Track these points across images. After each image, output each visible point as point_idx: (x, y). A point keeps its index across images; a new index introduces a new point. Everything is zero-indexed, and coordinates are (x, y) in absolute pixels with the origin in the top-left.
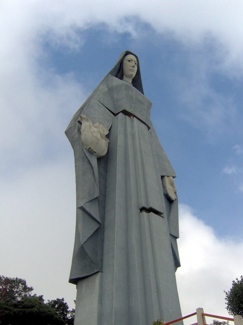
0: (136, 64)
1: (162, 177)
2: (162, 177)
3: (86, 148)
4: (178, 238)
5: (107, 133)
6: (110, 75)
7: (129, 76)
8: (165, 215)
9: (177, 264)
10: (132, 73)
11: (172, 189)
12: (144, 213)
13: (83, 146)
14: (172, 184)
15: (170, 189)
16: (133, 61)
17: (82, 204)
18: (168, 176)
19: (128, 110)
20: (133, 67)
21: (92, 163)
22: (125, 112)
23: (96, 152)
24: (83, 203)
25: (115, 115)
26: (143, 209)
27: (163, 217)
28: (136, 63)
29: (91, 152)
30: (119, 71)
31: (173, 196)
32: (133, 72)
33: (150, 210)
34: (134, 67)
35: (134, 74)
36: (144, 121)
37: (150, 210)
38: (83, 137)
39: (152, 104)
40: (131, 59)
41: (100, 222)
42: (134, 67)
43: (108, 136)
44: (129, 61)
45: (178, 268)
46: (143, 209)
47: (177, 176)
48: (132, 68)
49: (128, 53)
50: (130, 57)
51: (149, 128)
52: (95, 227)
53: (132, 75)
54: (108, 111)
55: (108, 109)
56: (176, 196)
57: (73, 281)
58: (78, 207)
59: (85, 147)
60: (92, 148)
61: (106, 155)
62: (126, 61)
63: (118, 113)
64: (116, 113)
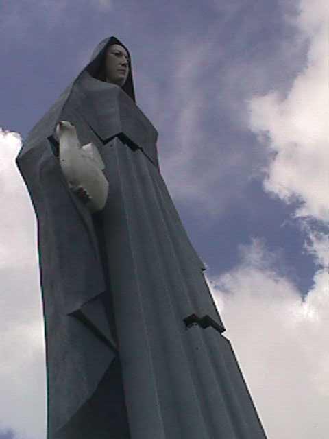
3: (71, 189)
6: (87, 74)
10: (123, 76)
12: (196, 328)
16: (124, 58)
20: (123, 65)
22: (122, 138)
25: (105, 142)
26: (189, 321)
29: (82, 196)
30: (99, 68)
32: (124, 74)
35: (125, 77)
44: (117, 54)
46: (189, 321)
48: (123, 68)
49: (113, 41)
50: (117, 48)
53: (122, 79)
60: (85, 190)
62: (112, 55)
63: (112, 138)
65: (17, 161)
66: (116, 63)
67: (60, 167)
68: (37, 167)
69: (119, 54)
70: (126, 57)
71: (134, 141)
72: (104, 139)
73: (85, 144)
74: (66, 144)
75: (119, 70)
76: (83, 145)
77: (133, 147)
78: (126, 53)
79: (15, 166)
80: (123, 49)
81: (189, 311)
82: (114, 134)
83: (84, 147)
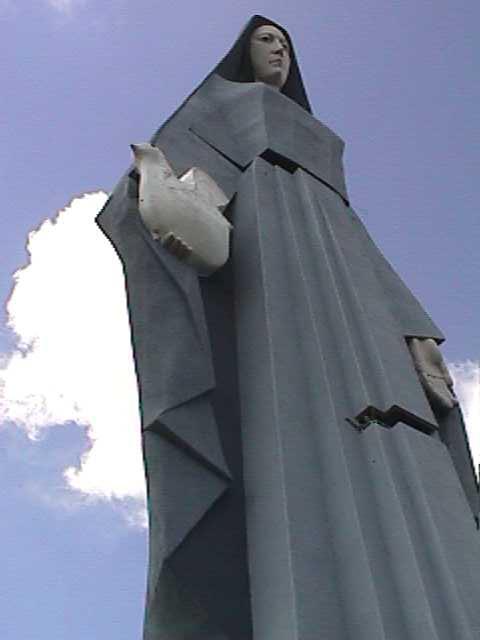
0: (284, 46)
1: (409, 339)
2: (409, 339)
3: (157, 240)
6: (216, 76)
7: (272, 80)
10: (278, 69)
11: (439, 375)
13: (149, 234)
14: (437, 363)
15: (434, 377)
16: (277, 41)
17: (155, 414)
18: (421, 339)
20: (277, 53)
21: (180, 282)
22: (270, 157)
23: (187, 250)
24: (162, 411)
28: (286, 43)
29: (175, 248)
30: (239, 64)
31: (447, 400)
32: (280, 65)
33: (394, 417)
37: (394, 417)
38: (145, 204)
39: (342, 144)
40: (270, 35)
42: (282, 55)
44: (265, 39)
47: (446, 337)
48: (277, 57)
49: (259, 21)
50: (266, 30)
52: (214, 490)
53: (278, 74)
54: (221, 157)
55: (220, 153)
56: (454, 395)
59: (155, 236)
61: (226, 265)
62: (260, 43)
66: (265, 53)
67: (137, 211)
69: (269, 39)
70: (281, 41)
71: (300, 158)
72: (244, 166)
74: (153, 175)
75: (270, 62)
77: (290, 166)
78: (283, 38)
80: (275, 28)
83: (183, 179)
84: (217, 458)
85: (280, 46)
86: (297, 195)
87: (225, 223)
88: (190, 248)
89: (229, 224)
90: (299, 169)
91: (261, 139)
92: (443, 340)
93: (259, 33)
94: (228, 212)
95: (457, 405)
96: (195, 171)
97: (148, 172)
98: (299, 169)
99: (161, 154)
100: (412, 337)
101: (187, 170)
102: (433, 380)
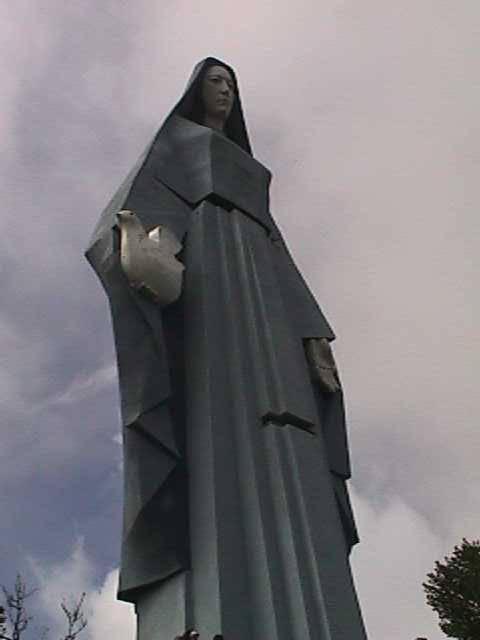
0: (230, 86)
1: (306, 342)
2: (306, 342)
4: (349, 476)
5: (178, 248)
6: (176, 117)
8: (317, 429)
9: (352, 538)
10: (223, 108)
11: (328, 366)
12: (271, 426)
14: (328, 355)
17: (134, 417)
19: (225, 193)
22: (213, 199)
24: (138, 415)
26: (268, 419)
27: (313, 433)
28: (231, 83)
29: (143, 293)
31: (332, 385)
32: (225, 102)
34: (226, 93)
35: (227, 109)
36: (256, 216)
37: (286, 419)
40: (219, 76)
41: (176, 452)
43: (180, 257)
45: (355, 547)
46: (268, 419)
48: (224, 97)
49: (211, 62)
50: (217, 71)
51: (268, 231)
53: (224, 112)
54: (177, 199)
57: (121, 596)
58: (127, 424)
62: (212, 84)
64: (190, 200)
65: (87, 255)
68: (103, 260)
70: (228, 82)
73: (152, 229)
75: (219, 101)
76: (148, 233)
77: (228, 206)
78: (229, 76)
79: (85, 259)
81: (266, 407)
82: (203, 196)
84: (171, 445)
85: (227, 88)
86: (230, 232)
87: (179, 268)
88: (156, 293)
89: (180, 264)
90: (235, 211)
91: (207, 182)
92: (333, 339)
93: (214, 73)
94: (180, 257)
95: (340, 392)
96: (160, 231)
97: (128, 236)
98: (235, 211)
99: (138, 220)
100: (309, 339)
101: (155, 228)
102: (322, 370)
